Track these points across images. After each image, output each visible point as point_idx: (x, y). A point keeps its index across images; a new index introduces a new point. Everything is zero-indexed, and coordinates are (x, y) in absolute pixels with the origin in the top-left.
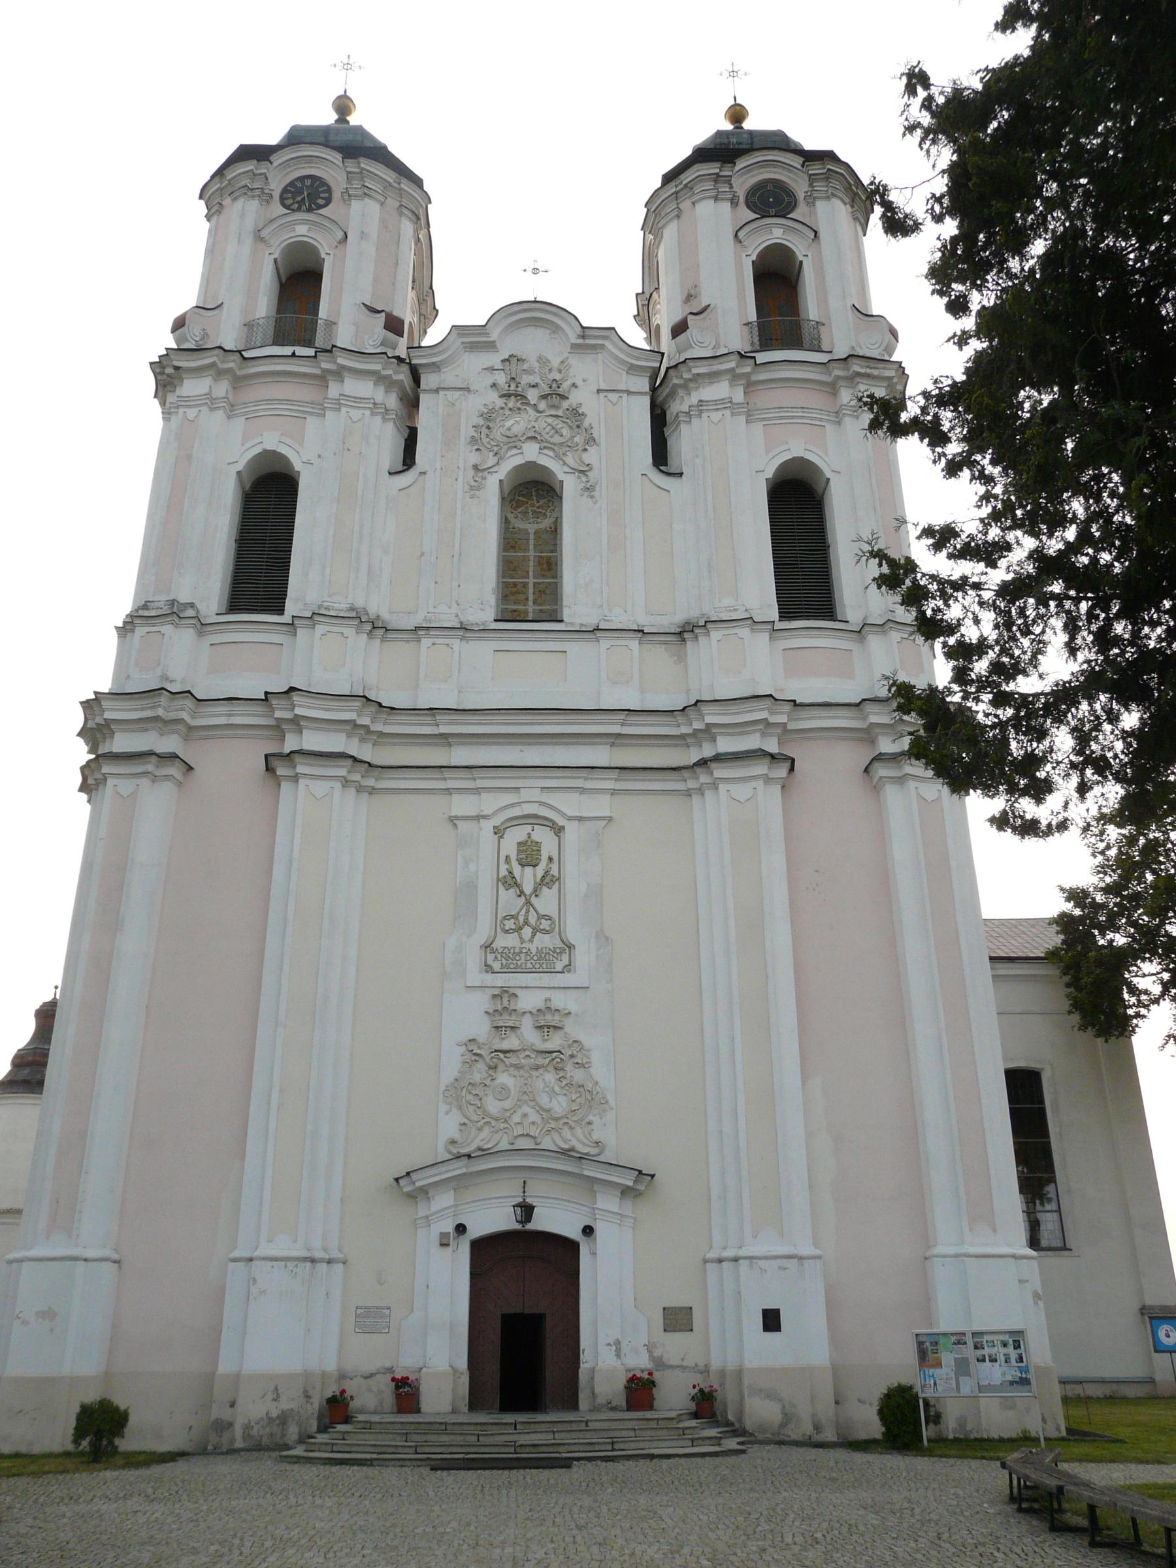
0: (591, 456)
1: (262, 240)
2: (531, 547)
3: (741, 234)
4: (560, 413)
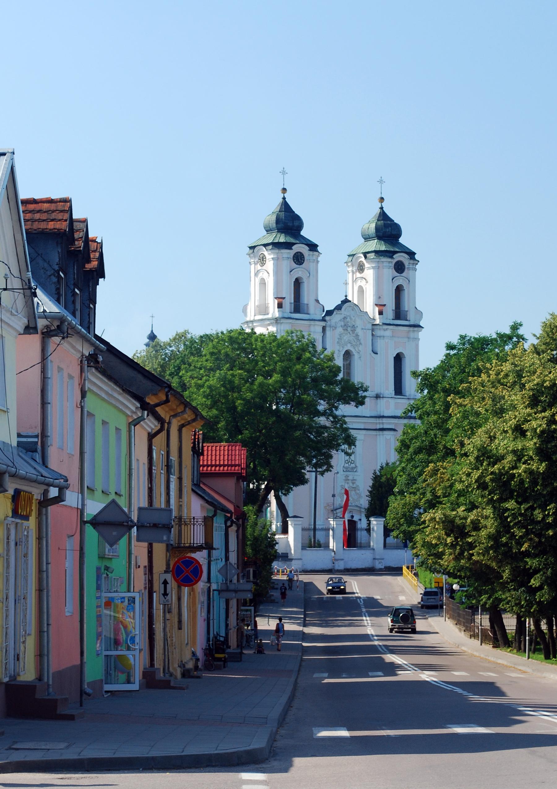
0: (361, 348)
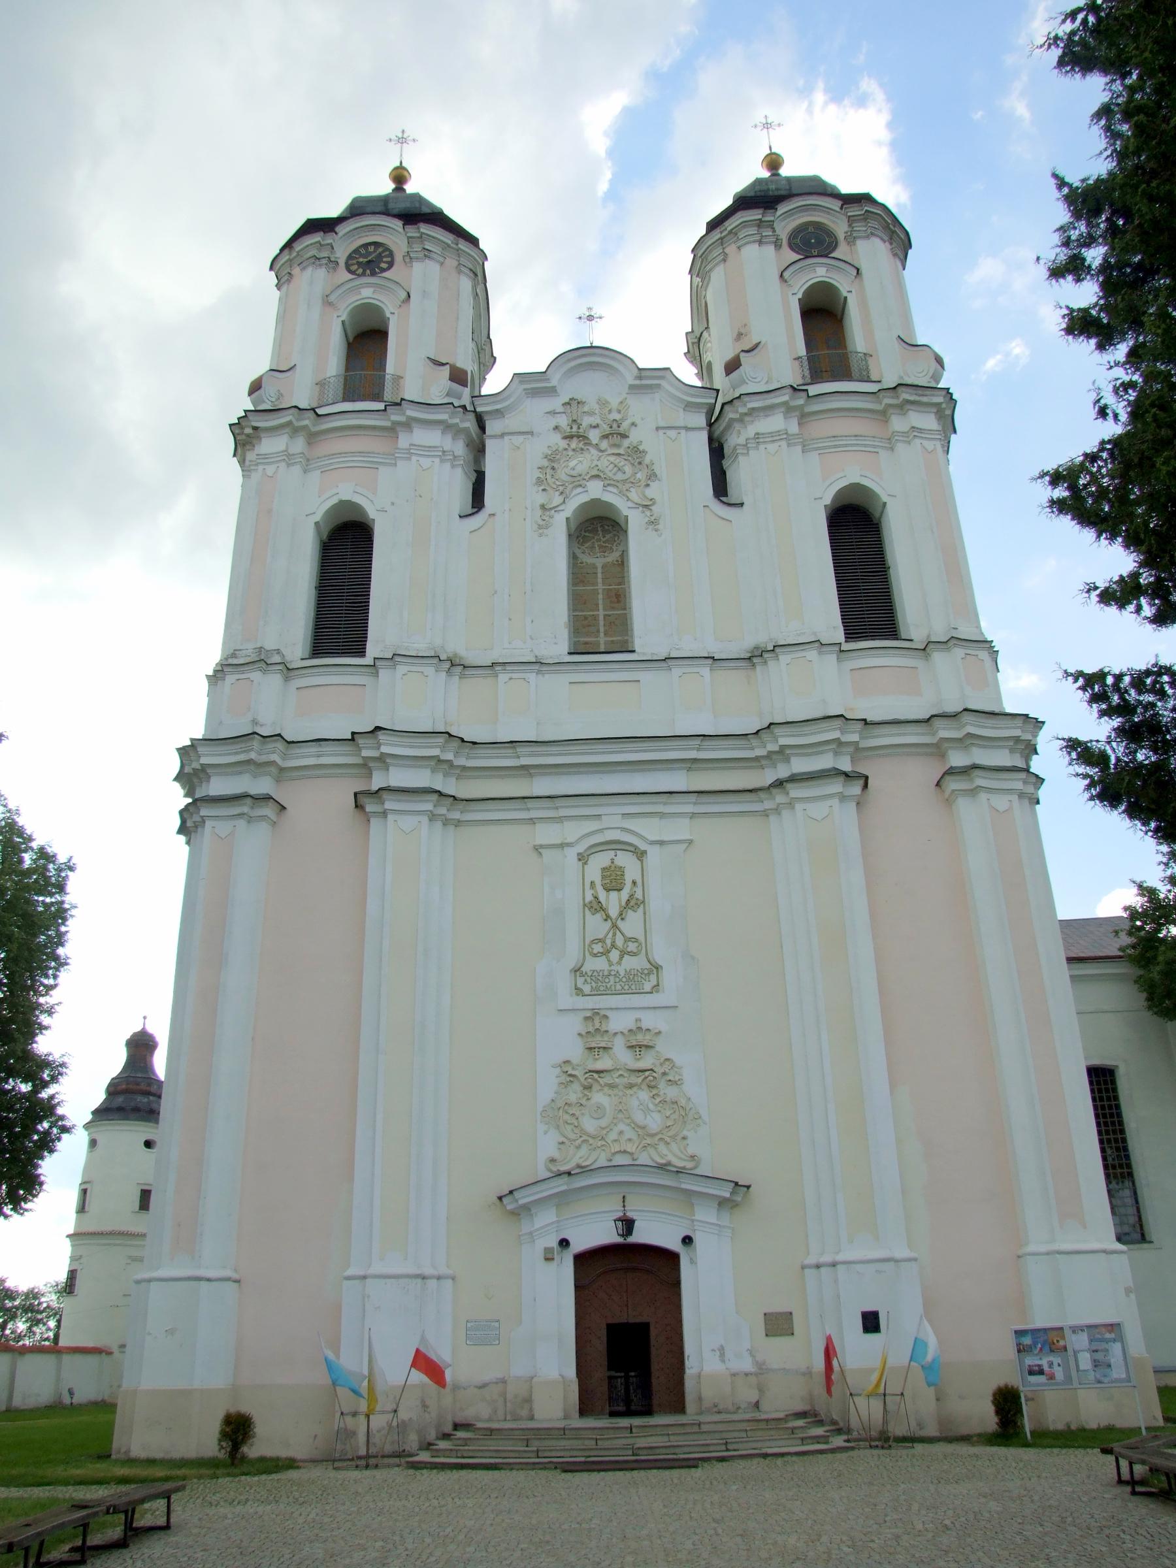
1: (330, 304)
2: (600, 580)
3: (786, 275)
4: (621, 451)
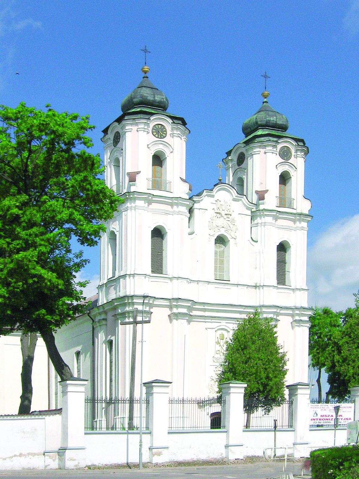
1: (149, 148)
2: (218, 256)
